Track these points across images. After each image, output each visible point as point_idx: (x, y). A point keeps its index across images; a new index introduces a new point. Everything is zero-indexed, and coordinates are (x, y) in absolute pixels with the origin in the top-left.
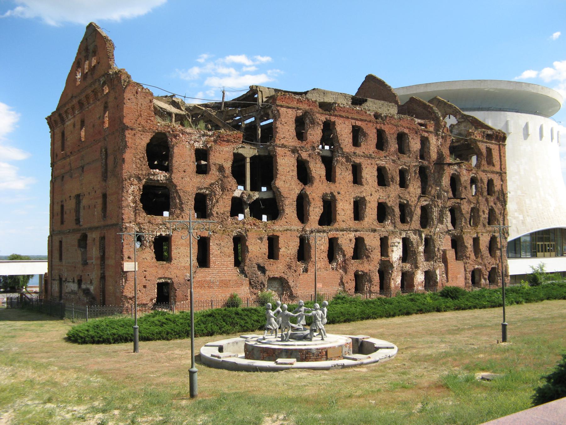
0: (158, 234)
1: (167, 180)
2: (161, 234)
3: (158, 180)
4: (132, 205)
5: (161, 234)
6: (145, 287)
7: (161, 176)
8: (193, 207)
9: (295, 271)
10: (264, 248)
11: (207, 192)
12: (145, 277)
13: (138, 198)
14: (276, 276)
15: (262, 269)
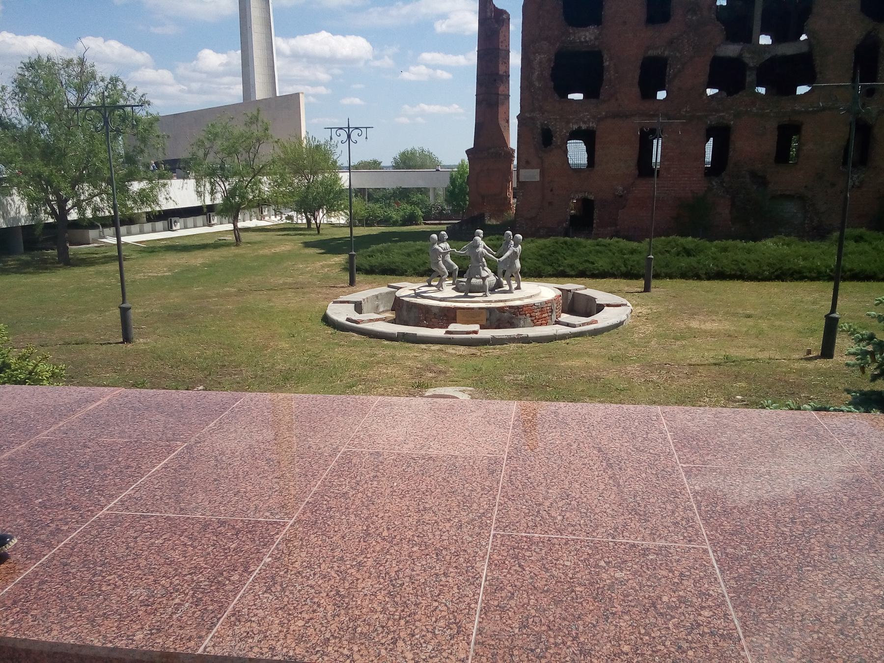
0: (575, 127)
1: (596, 39)
2: (580, 127)
3: (581, 42)
4: (537, 84)
5: (580, 127)
6: (550, 203)
7: (587, 35)
8: (636, 81)
9: (833, 185)
10: (770, 144)
11: (666, 53)
12: (552, 190)
13: (547, 73)
14: (788, 193)
15: (760, 180)
